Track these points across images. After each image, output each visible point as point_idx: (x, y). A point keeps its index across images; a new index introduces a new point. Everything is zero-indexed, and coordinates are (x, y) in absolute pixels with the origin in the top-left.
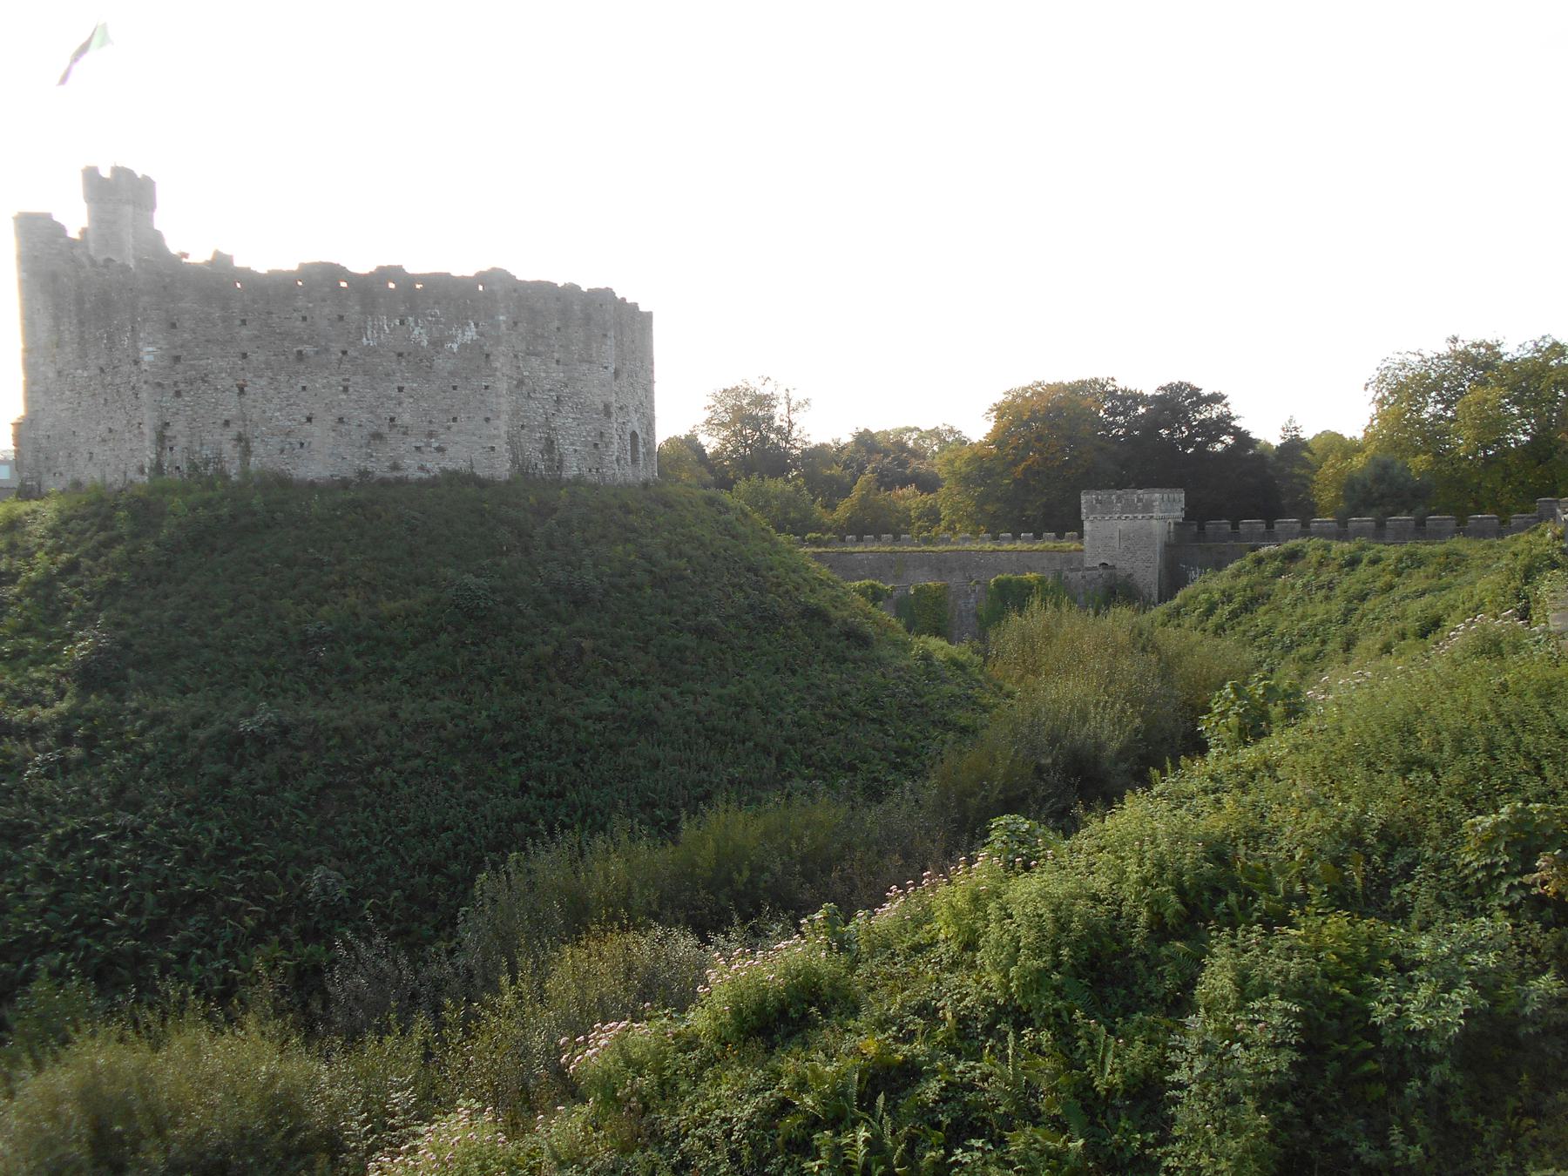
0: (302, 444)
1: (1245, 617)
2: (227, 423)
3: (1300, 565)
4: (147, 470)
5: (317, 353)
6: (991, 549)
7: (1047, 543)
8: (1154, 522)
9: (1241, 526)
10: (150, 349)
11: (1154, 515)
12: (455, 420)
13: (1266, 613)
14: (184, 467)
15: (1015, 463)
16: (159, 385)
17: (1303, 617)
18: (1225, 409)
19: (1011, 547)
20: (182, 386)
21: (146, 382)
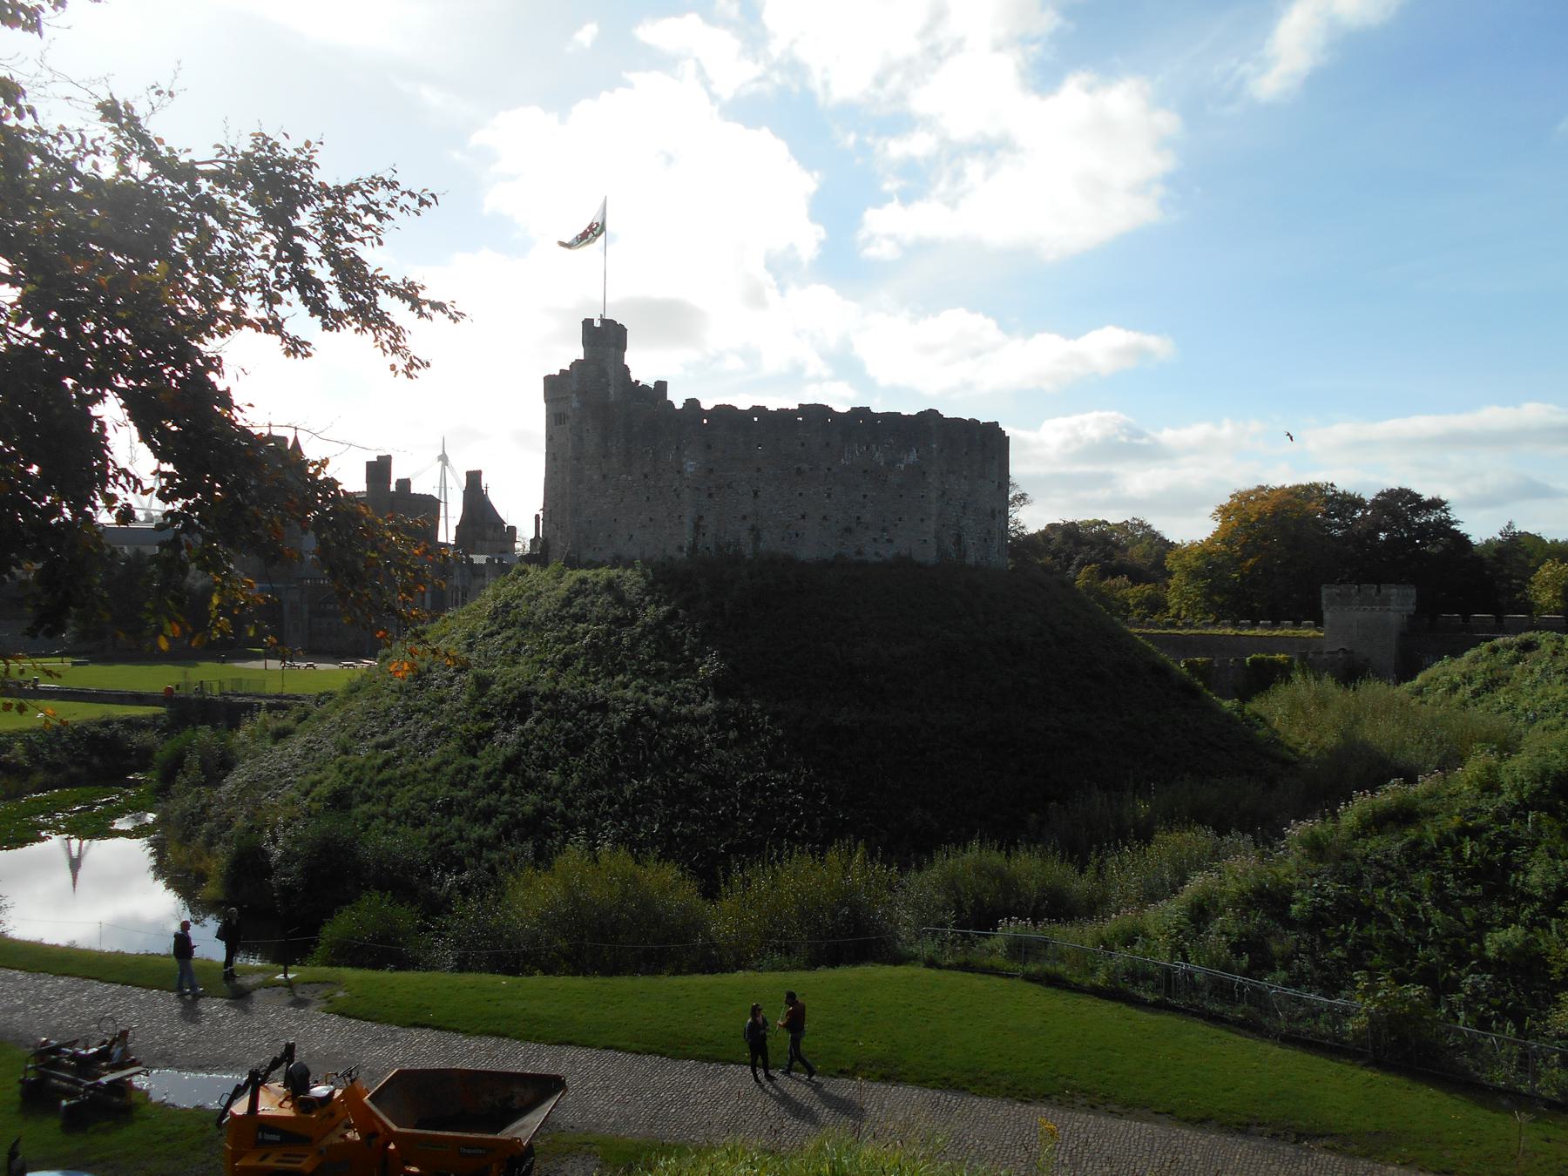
0: (797, 535)
1: (1486, 696)
2: (744, 517)
3: (1535, 653)
4: (685, 549)
5: (811, 469)
6: (1233, 634)
7: (1285, 630)
8: (1391, 613)
9: (1471, 620)
10: (692, 463)
11: (1391, 607)
12: (900, 520)
13: (1507, 693)
14: (712, 548)
15: (1243, 559)
16: (697, 489)
17: (1544, 696)
18: (1444, 514)
19: (1251, 632)
20: (713, 491)
21: (688, 487)
